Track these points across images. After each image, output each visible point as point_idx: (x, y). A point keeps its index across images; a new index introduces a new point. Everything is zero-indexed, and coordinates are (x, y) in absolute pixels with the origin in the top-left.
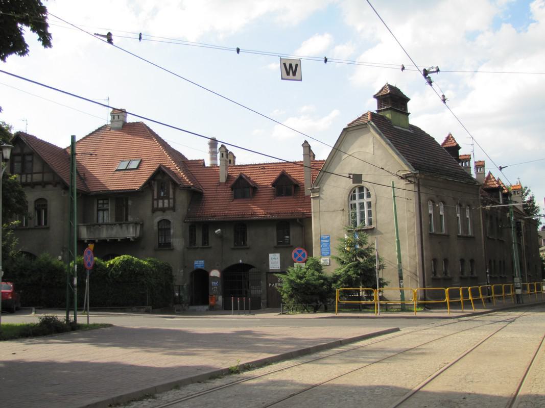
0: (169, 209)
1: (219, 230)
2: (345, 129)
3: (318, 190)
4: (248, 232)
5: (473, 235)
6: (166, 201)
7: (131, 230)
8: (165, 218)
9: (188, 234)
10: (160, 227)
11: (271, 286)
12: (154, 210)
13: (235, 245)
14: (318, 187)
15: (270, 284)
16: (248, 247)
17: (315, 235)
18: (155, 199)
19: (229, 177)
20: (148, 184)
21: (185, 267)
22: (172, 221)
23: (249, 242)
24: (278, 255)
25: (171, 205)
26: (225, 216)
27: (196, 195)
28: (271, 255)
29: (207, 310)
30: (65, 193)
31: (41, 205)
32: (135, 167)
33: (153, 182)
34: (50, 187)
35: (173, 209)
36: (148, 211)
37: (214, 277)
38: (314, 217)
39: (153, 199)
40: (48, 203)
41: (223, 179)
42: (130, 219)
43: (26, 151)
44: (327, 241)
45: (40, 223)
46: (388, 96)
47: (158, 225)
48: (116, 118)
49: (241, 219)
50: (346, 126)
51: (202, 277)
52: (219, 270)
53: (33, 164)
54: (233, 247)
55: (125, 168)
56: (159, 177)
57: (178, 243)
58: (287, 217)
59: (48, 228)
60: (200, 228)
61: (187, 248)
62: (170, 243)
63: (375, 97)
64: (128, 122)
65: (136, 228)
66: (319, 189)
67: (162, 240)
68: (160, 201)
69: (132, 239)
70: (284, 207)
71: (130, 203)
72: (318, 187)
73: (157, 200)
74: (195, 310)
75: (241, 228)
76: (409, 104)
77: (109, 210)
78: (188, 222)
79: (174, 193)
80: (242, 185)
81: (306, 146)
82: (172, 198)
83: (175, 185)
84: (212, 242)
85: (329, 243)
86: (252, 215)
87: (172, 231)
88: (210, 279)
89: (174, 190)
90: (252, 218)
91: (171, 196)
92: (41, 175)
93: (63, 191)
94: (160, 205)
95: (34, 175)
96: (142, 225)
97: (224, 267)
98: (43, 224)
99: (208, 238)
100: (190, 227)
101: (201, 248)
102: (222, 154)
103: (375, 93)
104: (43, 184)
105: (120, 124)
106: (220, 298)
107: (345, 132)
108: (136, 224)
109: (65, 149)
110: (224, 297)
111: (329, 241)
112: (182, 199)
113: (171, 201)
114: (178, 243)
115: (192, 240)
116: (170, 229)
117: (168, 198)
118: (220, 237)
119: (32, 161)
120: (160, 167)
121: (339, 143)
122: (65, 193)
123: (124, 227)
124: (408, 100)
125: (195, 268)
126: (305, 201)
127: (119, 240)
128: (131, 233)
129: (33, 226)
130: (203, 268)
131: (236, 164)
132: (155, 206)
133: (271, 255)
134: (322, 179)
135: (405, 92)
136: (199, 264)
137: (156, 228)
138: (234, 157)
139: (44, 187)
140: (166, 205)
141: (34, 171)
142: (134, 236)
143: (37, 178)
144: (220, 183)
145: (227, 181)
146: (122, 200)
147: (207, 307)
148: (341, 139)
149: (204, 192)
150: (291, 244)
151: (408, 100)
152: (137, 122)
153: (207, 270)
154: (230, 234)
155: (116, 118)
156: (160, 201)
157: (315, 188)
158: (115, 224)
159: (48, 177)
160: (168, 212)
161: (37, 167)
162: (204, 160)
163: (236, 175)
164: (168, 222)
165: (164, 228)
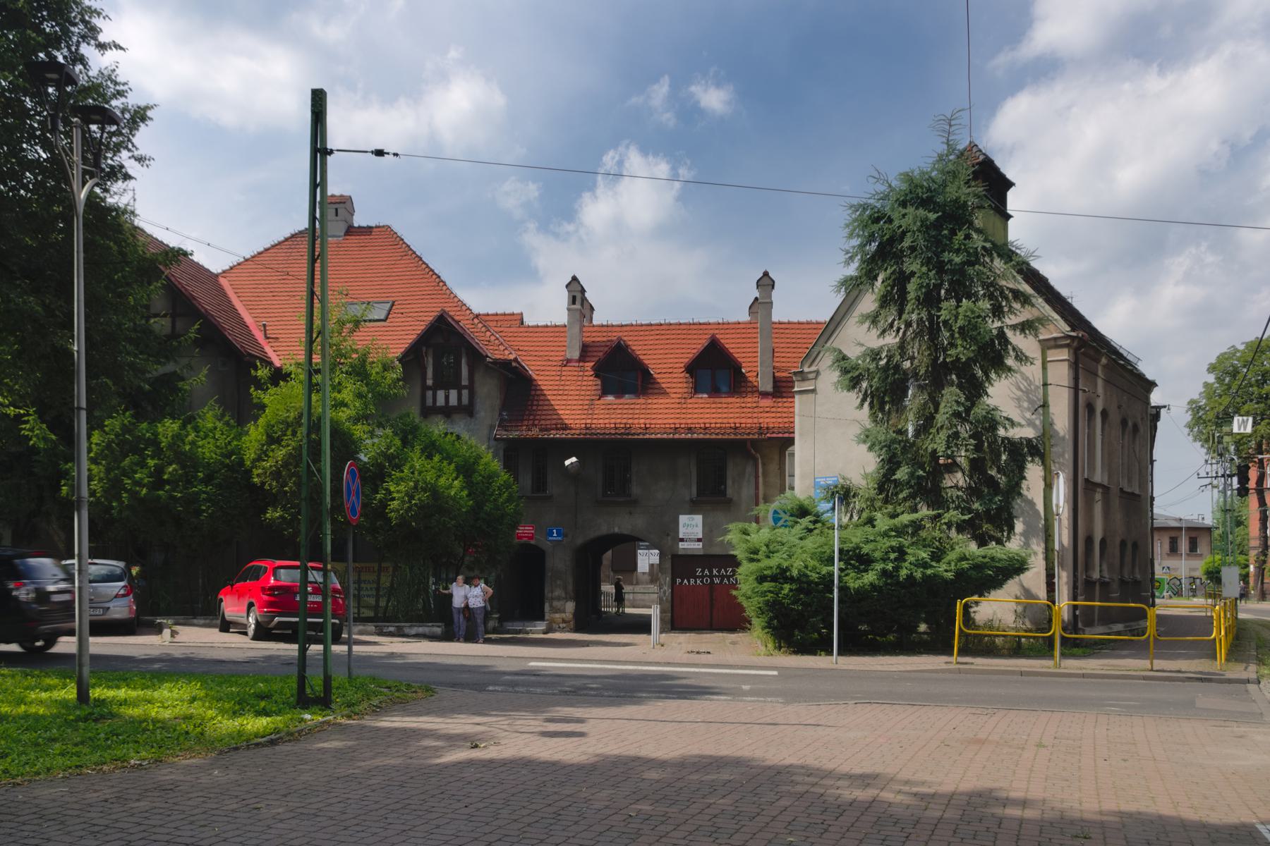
1: (574, 459)
5: (1137, 492)
6: (453, 394)
14: (813, 368)
15: (679, 581)
18: (429, 388)
23: (636, 490)
24: (698, 519)
25: (465, 400)
26: (587, 428)
28: (683, 519)
35: (468, 411)
38: (801, 435)
39: (425, 388)
64: (356, 225)
68: (441, 394)
72: (813, 368)
73: (435, 389)
75: (617, 458)
80: (617, 365)
82: (465, 387)
83: (476, 357)
91: (465, 382)
94: (441, 401)
109: (217, 276)
112: (488, 393)
113: (465, 393)
117: (459, 388)
131: (595, 322)
132: (429, 402)
133: (683, 519)
138: (592, 309)
140: (453, 401)
145: (581, 356)
156: (441, 394)
157: (806, 369)
160: (456, 417)
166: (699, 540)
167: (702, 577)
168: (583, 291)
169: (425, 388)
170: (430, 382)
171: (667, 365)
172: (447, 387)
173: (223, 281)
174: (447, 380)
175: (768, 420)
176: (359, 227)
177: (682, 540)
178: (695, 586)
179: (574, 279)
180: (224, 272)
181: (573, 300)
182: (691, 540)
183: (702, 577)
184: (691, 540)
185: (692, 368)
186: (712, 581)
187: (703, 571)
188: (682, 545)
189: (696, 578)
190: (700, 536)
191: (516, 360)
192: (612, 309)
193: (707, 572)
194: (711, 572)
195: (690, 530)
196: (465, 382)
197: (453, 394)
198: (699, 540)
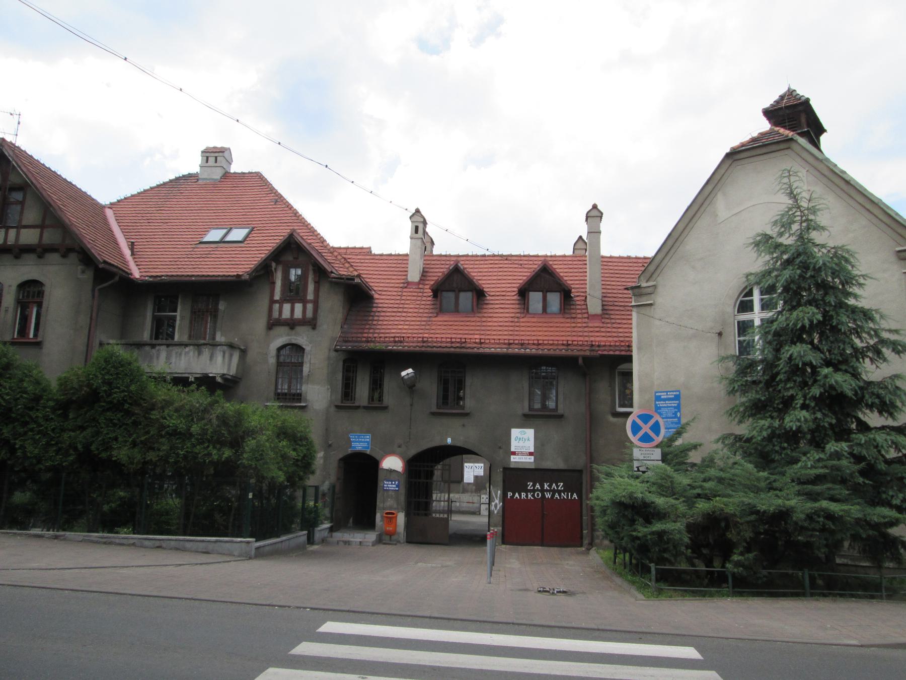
0: (303, 322)
1: (410, 371)
2: (728, 156)
3: (649, 290)
4: (468, 381)
6: (299, 307)
7: (219, 358)
8: (294, 342)
9: (340, 376)
10: (282, 359)
11: (512, 497)
12: (273, 324)
13: (438, 407)
14: (650, 283)
15: (510, 494)
16: (467, 410)
17: (641, 390)
18: (276, 302)
19: (424, 274)
20: (264, 271)
21: (330, 446)
22: (308, 349)
23: (469, 403)
24: (530, 433)
25: (309, 314)
26: (424, 342)
27: (357, 296)
28: (515, 433)
29: (374, 544)
30: (83, 272)
31: (31, 292)
32: (240, 239)
33: (274, 265)
34: (54, 257)
35: (311, 323)
37: (391, 471)
38: (639, 349)
39: (272, 302)
40: (47, 290)
41: (414, 275)
42: (219, 338)
43: (13, 179)
44: (674, 403)
45: (23, 331)
46: (801, 108)
47: (278, 356)
48: (212, 160)
49: (458, 350)
50: (728, 151)
51: (361, 471)
52: (401, 456)
53: (22, 209)
54: (434, 409)
55: (217, 239)
56: (289, 257)
57: (318, 394)
58: (558, 352)
59: (38, 344)
60: (368, 366)
61: (337, 407)
62: (300, 395)
64: (232, 171)
65: (231, 355)
66: (655, 286)
67: (284, 388)
68: (287, 307)
69: (219, 380)
70: (543, 333)
71: (222, 306)
72: (650, 283)
74: (347, 543)
75: (451, 370)
77: (178, 318)
78: (344, 351)
80: (455, 284)
81: (594, 215)
82: (310, 301)
83: (321, 273)
84: (391, 393)
85: (678, 408)
86: (481, 343)
87: (306, 369)
88: (381, 475)
89: (317, 283)
90: (481, 350)
91: (310, 296)
92: (38, 231)
93: (80, 267)
94: (286, 314)
95: (23, 231)
96: (243, 352)
97: (413, 452)
98: (31, 336)
99: (381, 386)
100: (344, 361)
101: (365, 407)
104: (40, 251)
105: (217, 174)
106: (401, 518)
107: (729, 162)
108: (231, 346)
109: (104, 207)
110: (407, 515)
111: (679, 405)
112: (332, 307)
113: (310, 307)
115: (348, 391)
116: (301, 364)
117: (304, 302)
118: (410, 386)
119: (22, 203)
120: (291, 235)
121: (710, 187)
122: (83, 272)
123: (206, 352)
125: (350, 451)
126: (590, 325)
128: (218, 365)
131: (435, 253)
132: (276, 315)
133: (515, 433)
134: (663, 264)
136: (361, 443)
137: (272, 361)
138: (432, 243)
139: (40, 257)
140: (298, 314)
141: (24, 223)
143: (29, 237)
144: (408, 283)
147: (371, 536)
148: (718, 177)
149: (376, 296)
150: (560, 412)
152: (250, 173)
154: (430, 386)
155: (212, 160)
157: (644, 285)
158: (186, 345)
159: (50, 237)
160: (299, 329)
161: (31, 215)
162: (370, 248)
163: (438, 273)
164: (298, 349)
165: (291, 360)
166: (531, 454)
167: (534, 491)
168: (425, 223)
169: (272, 302)
170: (277, 297)
171: (501, 289)
172: (293, 302)
173: (109, 213)
174: (294, 293)
175: (600, 338)
176: (235, 173)
177: (514, 453)
178: (527, 501)
179: (418, 211)
180: (111, 204)
181: (416, 230)
182: (522, 454)
183: (534, 491)
184: (522, 454)
185: (523, 293)
186: (543, 495)
187: (534, 485)
188: (513, 459)
189: (527, 491)
190: (532, 450)
191: (359, 276)
192: (450, 241)
193: (538, 486)
194: (542, 486)
195: (521, 444)
196: (310, 296)
197: (299, 307)
198: (531, 454)
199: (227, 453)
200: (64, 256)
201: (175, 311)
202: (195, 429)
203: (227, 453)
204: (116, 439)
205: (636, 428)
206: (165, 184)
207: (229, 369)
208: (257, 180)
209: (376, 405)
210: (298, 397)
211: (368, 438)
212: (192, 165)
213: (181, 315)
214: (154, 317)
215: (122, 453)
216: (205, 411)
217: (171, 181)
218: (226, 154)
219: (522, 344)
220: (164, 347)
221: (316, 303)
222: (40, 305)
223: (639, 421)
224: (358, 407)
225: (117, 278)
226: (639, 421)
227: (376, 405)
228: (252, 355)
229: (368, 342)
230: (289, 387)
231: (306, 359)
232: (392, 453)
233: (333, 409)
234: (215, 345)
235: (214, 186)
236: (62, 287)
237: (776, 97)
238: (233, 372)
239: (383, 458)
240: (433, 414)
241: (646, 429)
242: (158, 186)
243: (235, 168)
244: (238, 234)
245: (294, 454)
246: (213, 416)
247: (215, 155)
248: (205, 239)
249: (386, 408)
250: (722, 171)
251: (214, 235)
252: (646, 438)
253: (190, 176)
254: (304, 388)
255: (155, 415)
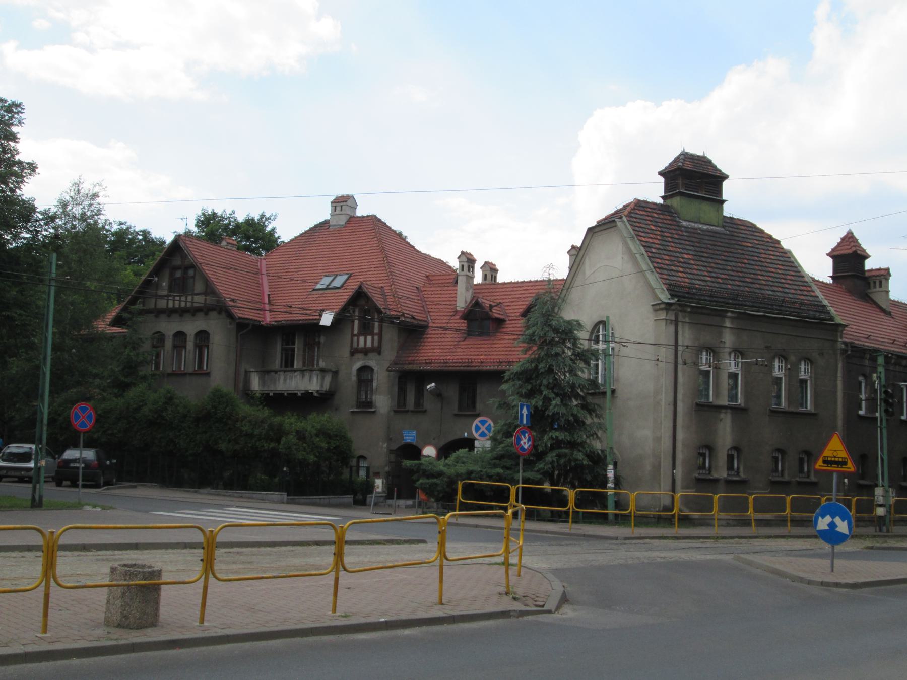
1: (433, 384)
2: (590, 230)
4: (478, 391)
5: (813, 411)
6: (369, 338)
9: (396, 389)
12: (354, 352)
13: (460, 408)
18: (355, 335)
21: (391, 439)
22: (376, 369)
25: (376, 344)
31: (203, 337)
34: (214, 314)
35: (378, 350)
36: (346, 352)
39: (353, 335)
46: (678, 172)
48: (338, 208)
49: (466, 368)
54: (456, 412)
57: (383, 402)
59: (208, 374)
61: (395, 411)
63: (661, 173)
65: (323, 378)
68: (362, 339)
69: (315, 394)
73: (358, 336)
76: (726, 184)
79: (381, 327)
87: (375, 384)
90: (481, 368)
91: (376, 331)
94: (362, 344)
96: (335, 373)
100: (399, 378)
101: (412, 411)
102: (463, 266)
103: (662, 168)
104: (205, 310)
105: (342, 221)
107: (590, 235)
108: (323, 371)
112: (391, 338)
113: (376, 338)
114: (383, 402)
116: (371, 381)
117: (372, 334)
119: (193, 277)
123: (307, 375)
124: (725, 177)
125: (403, 442)
127: (299, 394)
128: (313, 384)
129: (191, 370)
130: (414, 443)
132: (355, 345)
135: (720, 162)
136: (410, 437)
137: (354, 378)
139: (206, 314)
141: (196, 292)
142: (318, 389)
143: (199, 300)
144: (456, 312)
146: (298, 337)
151: (725, 177)
152: (368, 216)
153: (420, 447)
155: (338, 208)
156: (362, 339)
159: (210, 300)
160: (371, 355)
161: (199, 287)
169: (353, 335)
170: (356, 332)
172: (365, 335)
174: (366, 329)
196: (376, 331)
197: (369, 338)
199: (272, 445)
200: (220, 313)
201: (294, 344)
202: (256, 432)
203: (272, 445)
204: (220, 438)
205: (477, 428)
206: (306, 232)
207: (322, 386)
208: (373, 221)
209: (419, 409)
210: (370, 404)
211: (414, 433)
212: (324, 213)
213: (298, 346)
214: (283, 349)
215: (223, 446)
216: (262, 422)
217: (311, 229)
218: (349, 203)
219: (509, 362)
220: (282, 373)
221: (380, 335)
222: (208, 347)
223: (479, 424)
224: (408, 411)
225: (250, 327)
226: (479, 424)
227: (419, 409)
228: (342, 375)
229: (409, 364)
230: (366, 397)
231: (375, 377)
232: (430, 444)
233: (392, 413)
234: (312, 371)
235: (340, 230)
236: (220, 335)
237: (672, 159)
238: (326, 386)
239: (424, 447)
240: (456, 415)
241: (483, 429)
242: (301, 235)
243: (360, 212)
244: (339, 281)
245: (324, 445)
246: (266, 426)
247: (342, 203)
248: (319, 286)
249: (425, 411)
250: (587, 241)
251: (325, 281)
252: (483, 435)
253: (326, 223)
254: (374, 398)
255: (238, 424)
